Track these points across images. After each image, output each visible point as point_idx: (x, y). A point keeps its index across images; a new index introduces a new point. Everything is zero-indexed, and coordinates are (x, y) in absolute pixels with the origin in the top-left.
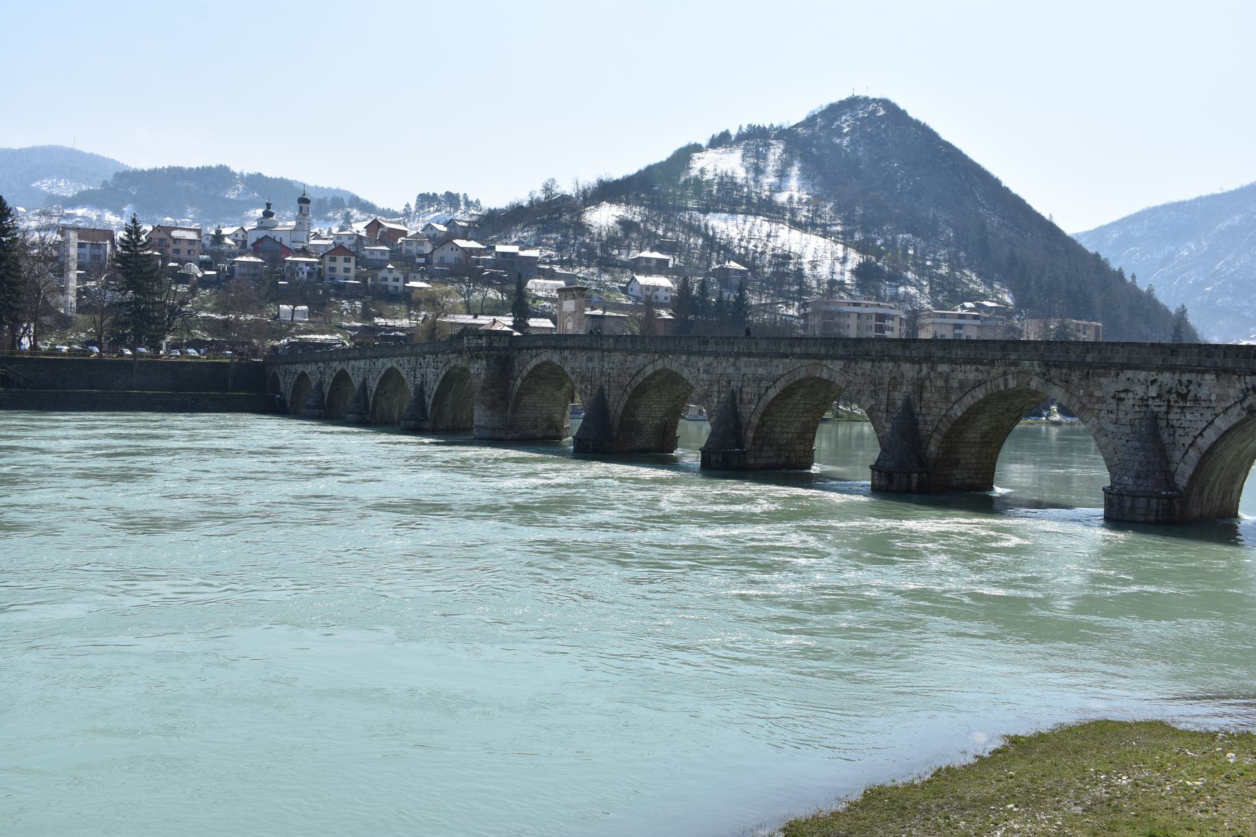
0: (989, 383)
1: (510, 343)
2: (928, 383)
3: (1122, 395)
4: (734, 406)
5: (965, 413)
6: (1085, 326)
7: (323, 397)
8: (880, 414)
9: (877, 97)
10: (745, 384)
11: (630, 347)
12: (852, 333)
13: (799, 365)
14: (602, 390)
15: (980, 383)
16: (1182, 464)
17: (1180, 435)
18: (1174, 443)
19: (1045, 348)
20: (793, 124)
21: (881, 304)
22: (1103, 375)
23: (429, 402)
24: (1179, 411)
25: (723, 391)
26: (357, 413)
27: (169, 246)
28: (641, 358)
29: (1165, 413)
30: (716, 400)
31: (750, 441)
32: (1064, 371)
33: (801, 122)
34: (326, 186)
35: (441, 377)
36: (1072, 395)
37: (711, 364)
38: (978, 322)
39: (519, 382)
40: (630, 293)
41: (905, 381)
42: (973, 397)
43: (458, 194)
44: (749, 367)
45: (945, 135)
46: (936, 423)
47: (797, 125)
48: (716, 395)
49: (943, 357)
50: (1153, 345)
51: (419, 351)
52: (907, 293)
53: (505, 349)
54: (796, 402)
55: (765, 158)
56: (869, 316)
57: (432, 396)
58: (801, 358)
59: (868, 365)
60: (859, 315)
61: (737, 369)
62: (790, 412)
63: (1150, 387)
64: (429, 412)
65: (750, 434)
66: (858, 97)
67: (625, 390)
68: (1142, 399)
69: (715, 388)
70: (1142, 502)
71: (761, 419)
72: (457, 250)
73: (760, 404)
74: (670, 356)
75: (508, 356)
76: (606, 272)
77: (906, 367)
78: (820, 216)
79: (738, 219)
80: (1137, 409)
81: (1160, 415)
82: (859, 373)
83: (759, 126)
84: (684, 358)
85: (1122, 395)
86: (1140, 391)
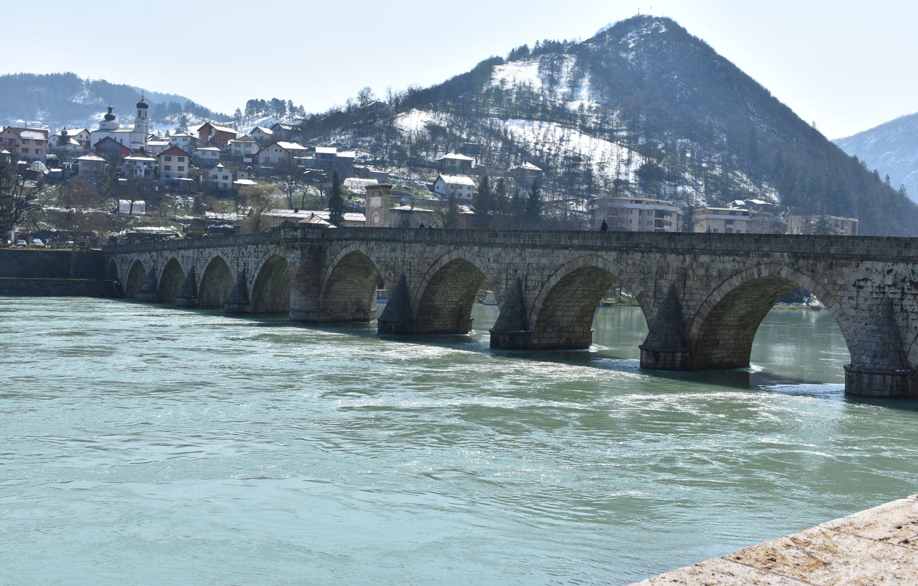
0: (744, 272)
1: (323, 236)
2: (690, 272)
3: (862, 284)
4: (520, 292)
5: (723, 299)
6: (843, 221)
7: (156, 283)
8: (648, 300)
9: (660, 16)
10: (530, 272)
11: (429, 239)
12: (635, 228)
13: (577, 255)
14: (403, 277)
15: (736, 272)
17: (913, 319)
18: (907, 327)
19: (794, 241)
20: (584, 39)
21: (660, 201)
22: (846, 266)
23: (250, 287)
24: (912, 297)
25: (510, 279)
26: (186, 297)
27: (18, 146)
28: (438, 249)
29: (899, 299)
30: (504, 287)
31: (534, 324)
32: (811, 262)
33: (592, 39)
34: (164, 93)
35: (261, 265)
36: (817, 283)
37: (500, 255)
38: (747, 218)
39: (330, 269)
40: (436, 190)
41: (670, 270)
42: (730, 285)
43: (283, 101)
44: (534, 258)
45: (720, 51)
46: (697, 308)
47: (588, 41)
48: (504, 282)
49: (704, 249)
50: (889, 238)
51: (241, 242)
52: (684, 192)
53: (318, 240)
54: (575, 288)
55: (559, 70)
56: (649, 212)
57: (253, 283)
58: (579, 249)
59: (638, 256)
60: (641, 211)
61: (522, 259)
62: (570, 297)
63: (886, 276)
64: (250, 296)
65: (534, 317)
66: (643, 16)
67: (424, 278)
68: (879, 287)
69: (504, 276)
70: (878, 379)
71: (544, 304)
72: (281, 151)
73: (543, 291)
74: (464, 248)
75: (321, 247)
76: (415, 171)
77: (671, 258)
78: (608, 123)
79: (534, 125)
80: (875, 296)
81: (895, 301)
82: (630, 263)
83: (554, 42)
84: (476, 249)
85: (862, 284)
86: (877, 279)
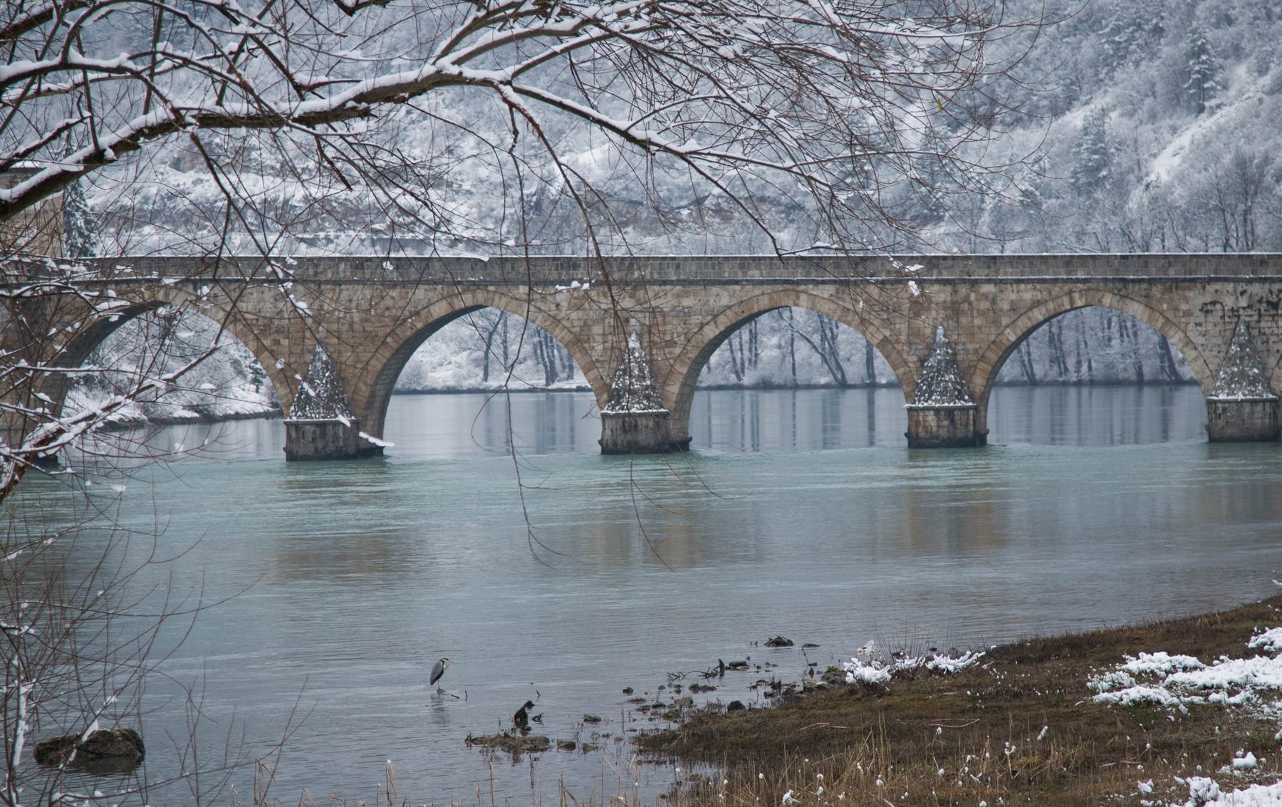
8: (898, 347)
15: (1036, 304)
16: (1277, 369)
18: (1268, 350)
22: (1190, 289)
28: (421, 293)
30: (599, 348)
42: (1029, 319)
48: (599, 338)
67: (384, 343)
68: (1232, 310)
74: (491, 288)
80: (1227, 319)
81: (1252, 324)
84: (523, 290)
85: (1209, 307)
86: (1229, 302)
